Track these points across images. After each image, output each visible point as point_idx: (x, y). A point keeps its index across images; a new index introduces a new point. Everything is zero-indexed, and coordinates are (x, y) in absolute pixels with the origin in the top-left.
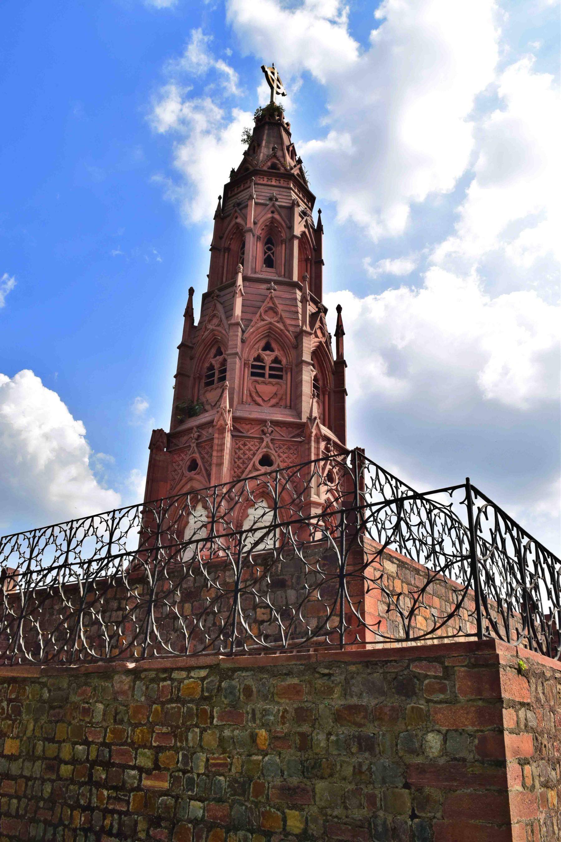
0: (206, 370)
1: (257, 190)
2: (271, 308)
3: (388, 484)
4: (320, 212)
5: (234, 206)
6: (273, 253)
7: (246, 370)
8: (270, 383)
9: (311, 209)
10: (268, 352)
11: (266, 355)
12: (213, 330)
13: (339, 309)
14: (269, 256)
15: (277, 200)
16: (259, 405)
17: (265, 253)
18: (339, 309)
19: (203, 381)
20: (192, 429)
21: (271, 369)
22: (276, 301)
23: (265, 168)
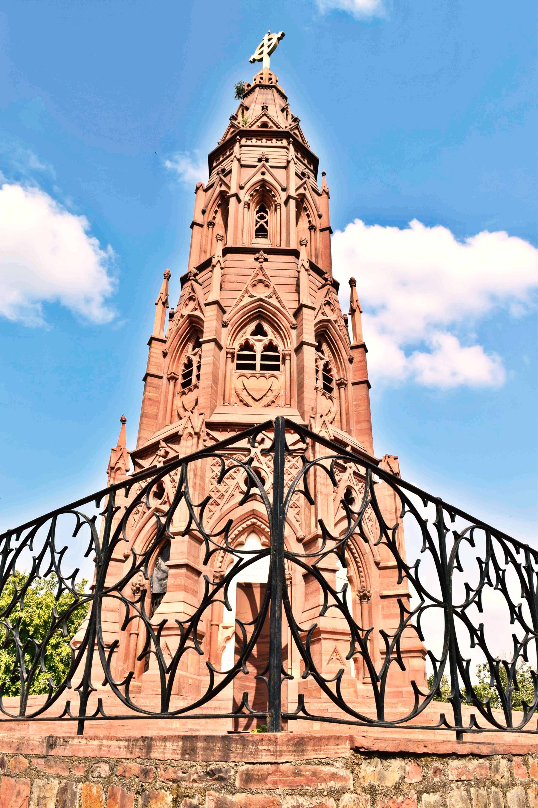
0: (183, 368)
1: (242, 152)
2: (261, 281)
3: (409, 517)
4: (324, 174)
5: (218, 174)
6: (266, 222)
7: (229, 360)
8: (263, 376)
9: (315, 172)
10: (259, 337)
11: (256, 340)
12: (189, 316)
13: (352, 283)
14: (262, 225)
15: (267, 160)
16: (246, 405)
17: (257, 222)
18: (352, 283)
19: (181, 380)
20: (158, 443)
21: (263, 358)
22: (269, 273)
23: (254, 128)
